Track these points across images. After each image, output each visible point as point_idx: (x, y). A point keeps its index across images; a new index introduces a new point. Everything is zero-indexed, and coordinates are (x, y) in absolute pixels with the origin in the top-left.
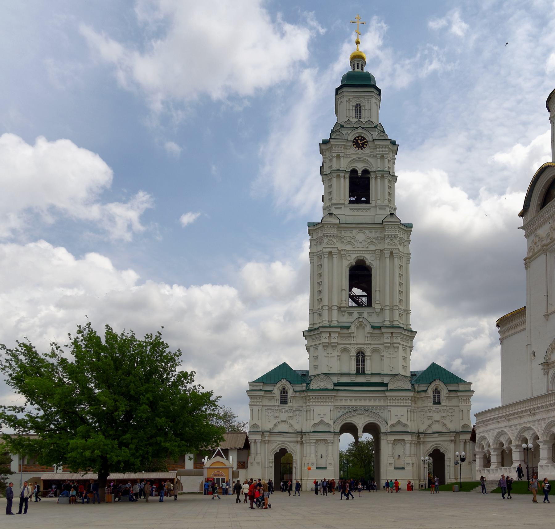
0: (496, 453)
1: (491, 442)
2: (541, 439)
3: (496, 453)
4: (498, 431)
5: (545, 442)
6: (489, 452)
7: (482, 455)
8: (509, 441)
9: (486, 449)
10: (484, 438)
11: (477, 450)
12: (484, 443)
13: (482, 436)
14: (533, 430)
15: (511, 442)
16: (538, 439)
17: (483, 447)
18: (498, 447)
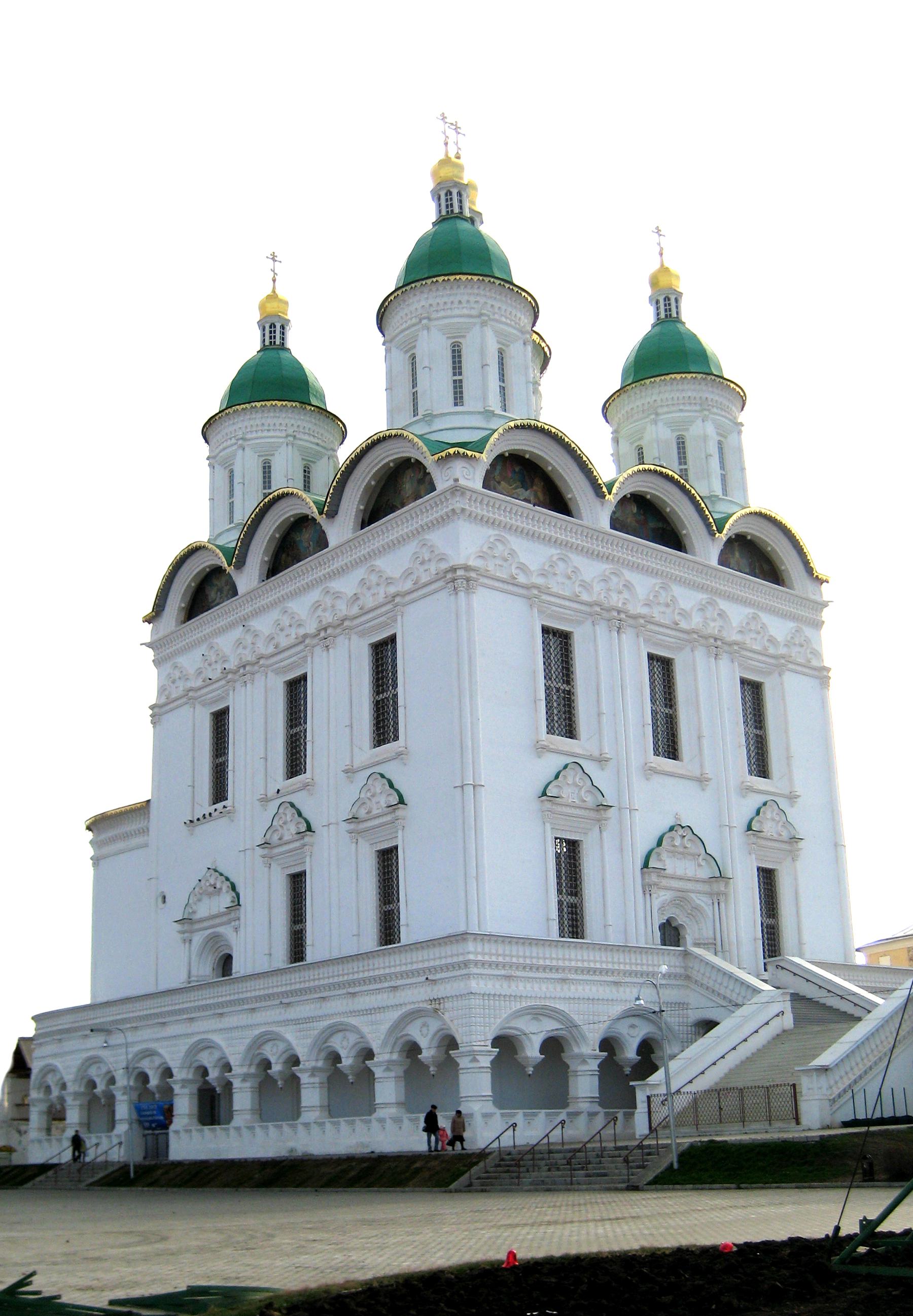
0: (78, 1102)
1: (68, 1077)
2: (236, 1070)
3: (78, 1102)
4: (85, 1055)
5: (245, 1078)
6: (62, 1100)
7: (43, 1107)
8: (108, 1077)
9: (55, 1092)
10: (50, 1070)
11: (34, 1094)
12: (51, 1080)
13: (48, 1065)
14: (159, 1054)
15: (112, 1081)
16: (230, 1070)
17: (48, 1089)
18: (82, 1089)
